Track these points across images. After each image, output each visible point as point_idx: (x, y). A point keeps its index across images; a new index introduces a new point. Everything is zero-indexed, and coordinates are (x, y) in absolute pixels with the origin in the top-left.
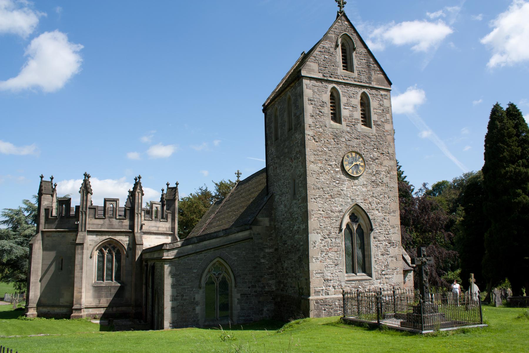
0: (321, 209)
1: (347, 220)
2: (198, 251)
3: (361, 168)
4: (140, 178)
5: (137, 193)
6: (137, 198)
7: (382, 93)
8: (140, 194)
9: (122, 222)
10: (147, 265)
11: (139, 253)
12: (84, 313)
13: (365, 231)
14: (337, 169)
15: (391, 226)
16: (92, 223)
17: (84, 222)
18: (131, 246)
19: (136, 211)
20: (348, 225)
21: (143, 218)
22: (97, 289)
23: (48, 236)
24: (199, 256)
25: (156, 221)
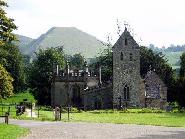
1: (124, 86)
23: (56, 83)
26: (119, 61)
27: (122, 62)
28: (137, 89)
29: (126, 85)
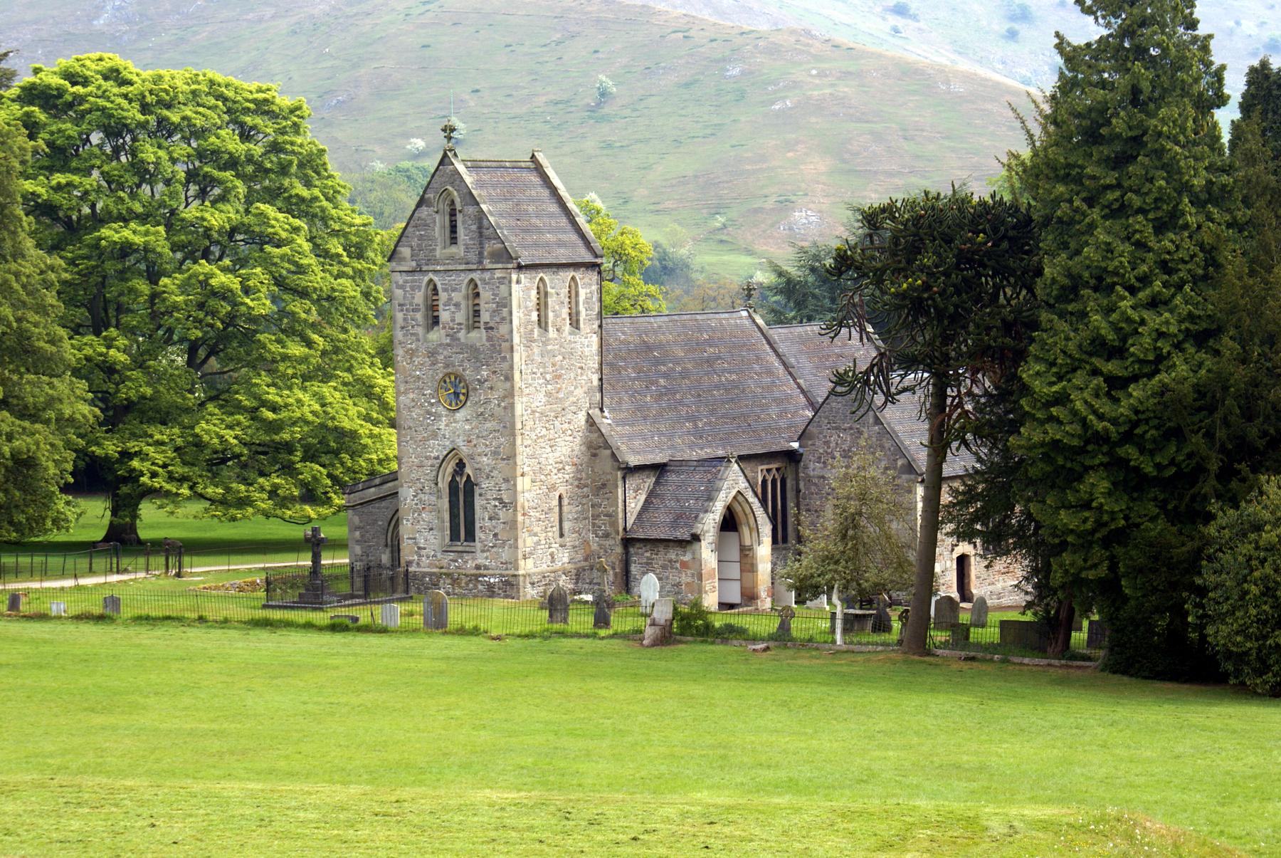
1: (450, 468)
3: (462, 398)
24: (383, 504)
26: (420, 331)
27: (436, 335)
28: (504, 486)
29: (461, 465)
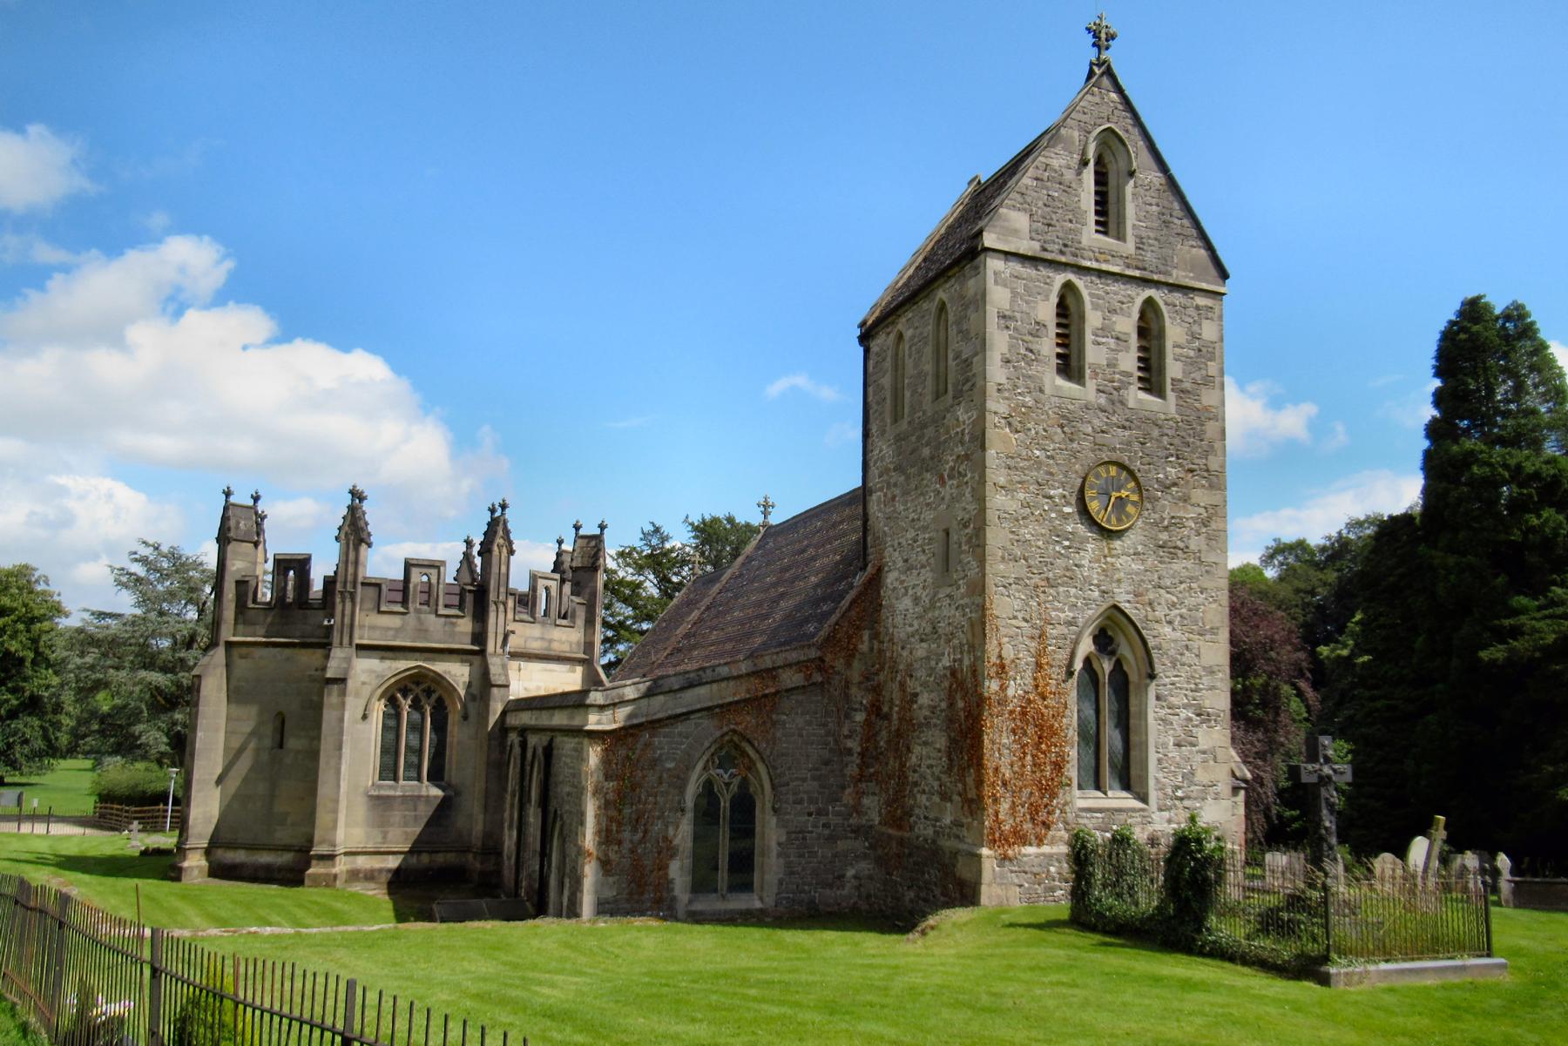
0: (1020, 615)
1: (1086, 646)
2: (679, 711)
3: (1130, 509)
4: (504, 507)
5: (495, 548)
6: (495, 560)
7: (1201, 301)
8: (505, 550)
9: (454, 624)
10: (524, 745)
11: (497, 708)
12: (341, 866)
13: (1133, 677)
14: (1068, 510)
15: (1204, 668)
16: (372, 625)
17: (347, 620)
18: (475, 690)
19: (492, 596)
20: (1088, 661)
21: (510, 615)
22: (380, 803)
23: (242, 657)
25: (543, 624)
